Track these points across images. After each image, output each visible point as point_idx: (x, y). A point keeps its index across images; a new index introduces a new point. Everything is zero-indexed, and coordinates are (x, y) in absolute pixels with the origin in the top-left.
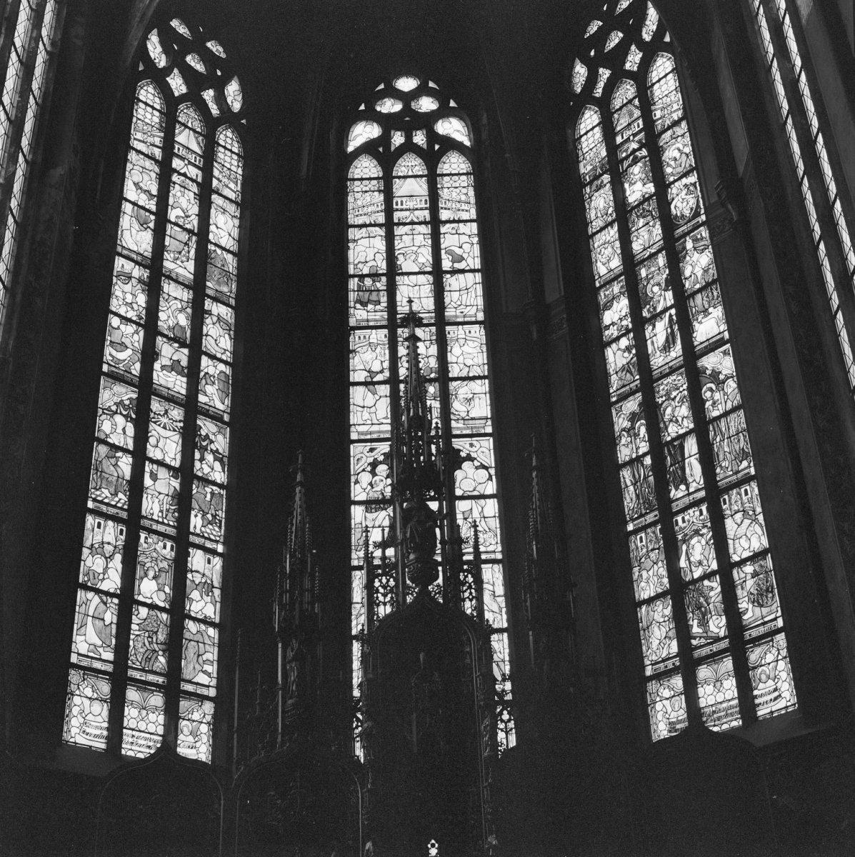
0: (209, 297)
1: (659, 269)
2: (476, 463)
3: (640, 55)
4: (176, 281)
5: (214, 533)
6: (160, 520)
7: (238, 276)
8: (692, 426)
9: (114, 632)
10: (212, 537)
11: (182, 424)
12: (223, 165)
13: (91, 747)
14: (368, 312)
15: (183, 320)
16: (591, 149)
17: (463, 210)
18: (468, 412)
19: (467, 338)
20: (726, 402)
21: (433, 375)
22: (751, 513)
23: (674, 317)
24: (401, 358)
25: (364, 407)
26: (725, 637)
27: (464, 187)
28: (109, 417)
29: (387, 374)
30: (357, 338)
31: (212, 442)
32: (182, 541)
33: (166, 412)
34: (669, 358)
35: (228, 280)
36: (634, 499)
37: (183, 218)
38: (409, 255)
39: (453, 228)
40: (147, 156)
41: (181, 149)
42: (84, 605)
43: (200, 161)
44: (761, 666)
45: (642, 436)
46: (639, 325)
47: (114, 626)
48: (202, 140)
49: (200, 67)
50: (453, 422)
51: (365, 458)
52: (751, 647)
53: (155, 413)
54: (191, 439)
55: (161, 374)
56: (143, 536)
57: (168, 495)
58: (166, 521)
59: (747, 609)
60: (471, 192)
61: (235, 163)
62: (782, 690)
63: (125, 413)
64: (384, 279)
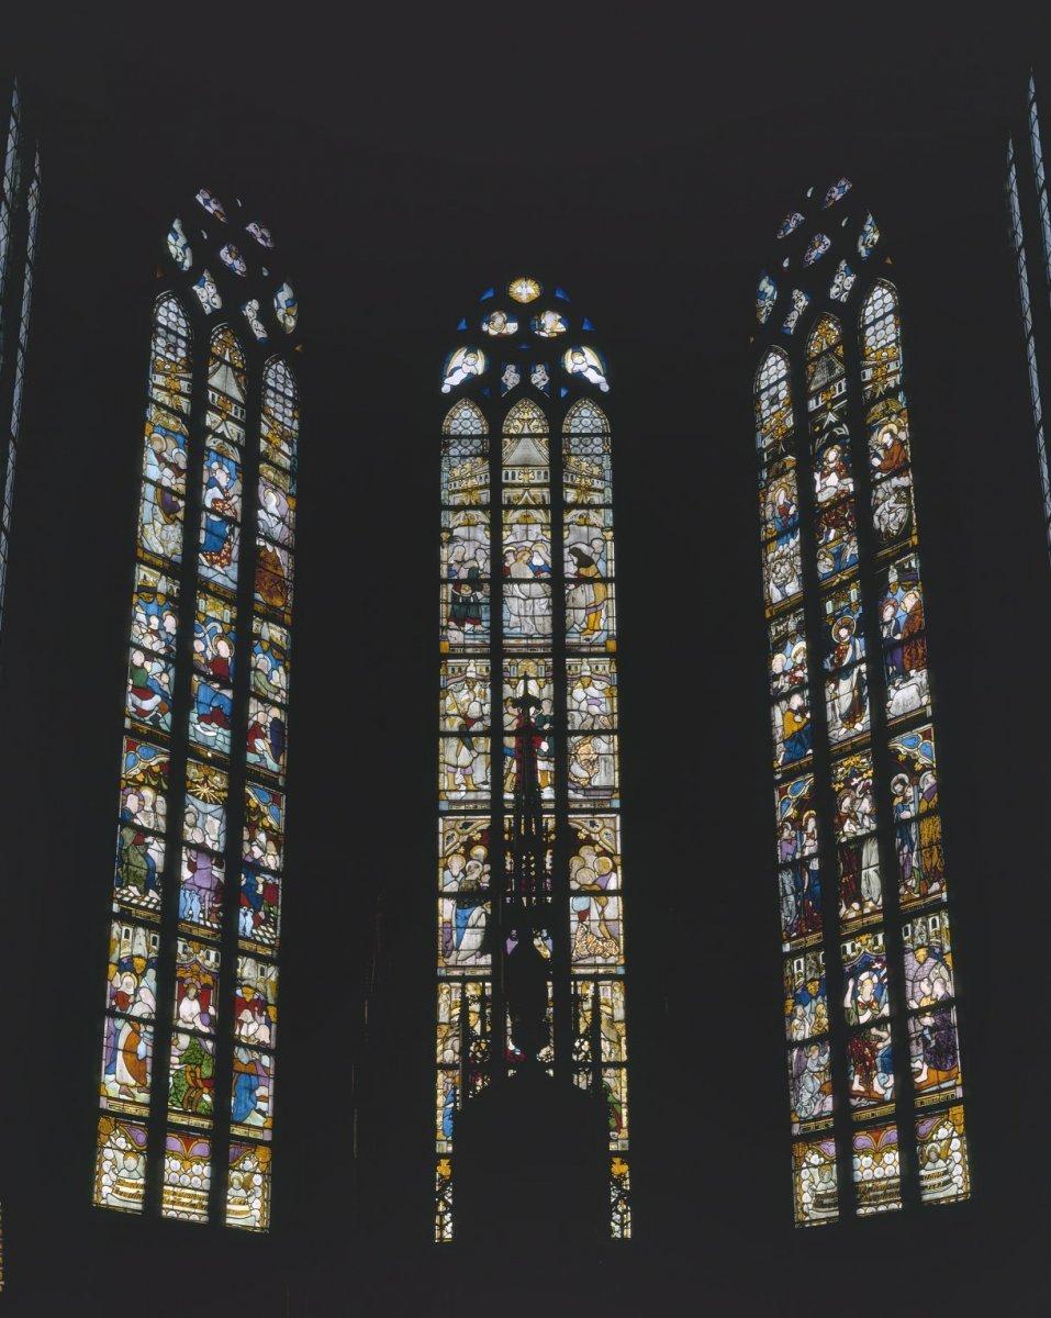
0: (258, 615)
1: (850, 605)
2: (598, 849)
3: (851, 279)
4: (215, 595)
5: (268, 935)
6: (202, 922)
7: (294, 581)
8: (874, 827)
9: (149, 1068)
10: (266, 941)
11: (225, 794)
12: (273, 418)
13: (126, 1209)
14: (465, 633)
15: (224, 650)
16: (773, 414)
17: (595, 490)
18: (590, 778)
19: (594, 676)
20: (920, 802)
21: (546, 727)
22: (937, 951)
23: (864, 676)
24: (506, 701)
25: (456, 767)
26: (891, 1101)
27: (598, 455)
28: (134, 790)
29: (488, 722)
30: (450, 672)
31: (264, 816)
32: (229, 944)
33: (206, 777)
34: (853, 731)
35: (282, 589)
36: (794, 912)
37: (221, 501)
38: (521, 554)
39: (581, 516)
40: (170, 410)
41: (217, 396)
42: (112, 1037)
43: (242, 413)
44: (933, 1141)
45: (810, 830)
46: (818, 680)
47: (149, 1061)
48: (245, 381)
49: (239, 267)
50: (571, 792)
51: (456, 835)
52: (921, 1118)
53: (192, 782)
54: (238, 817)
55: (198, 727)
56: (180, 944)
57: (209, 889)
58: (208, 924)
59: (921, 1070)
60: (607, 463)
61: (290, 414)
62: (954, 1173)
63: (154, 783)
64: (487, 587)
